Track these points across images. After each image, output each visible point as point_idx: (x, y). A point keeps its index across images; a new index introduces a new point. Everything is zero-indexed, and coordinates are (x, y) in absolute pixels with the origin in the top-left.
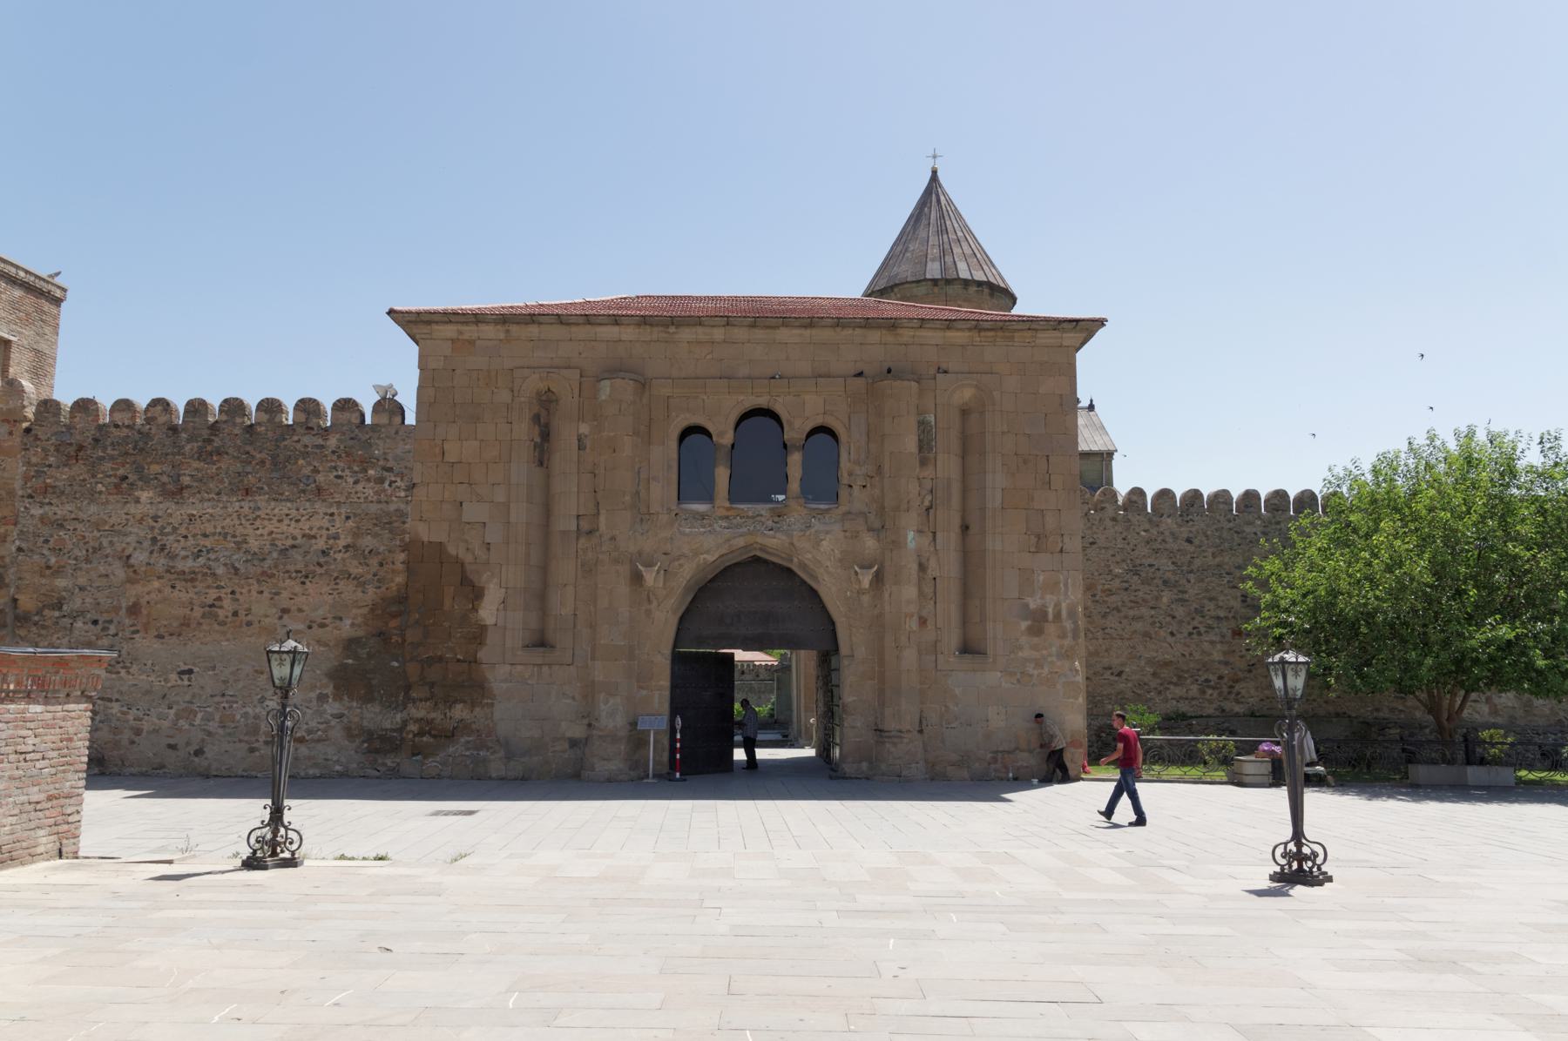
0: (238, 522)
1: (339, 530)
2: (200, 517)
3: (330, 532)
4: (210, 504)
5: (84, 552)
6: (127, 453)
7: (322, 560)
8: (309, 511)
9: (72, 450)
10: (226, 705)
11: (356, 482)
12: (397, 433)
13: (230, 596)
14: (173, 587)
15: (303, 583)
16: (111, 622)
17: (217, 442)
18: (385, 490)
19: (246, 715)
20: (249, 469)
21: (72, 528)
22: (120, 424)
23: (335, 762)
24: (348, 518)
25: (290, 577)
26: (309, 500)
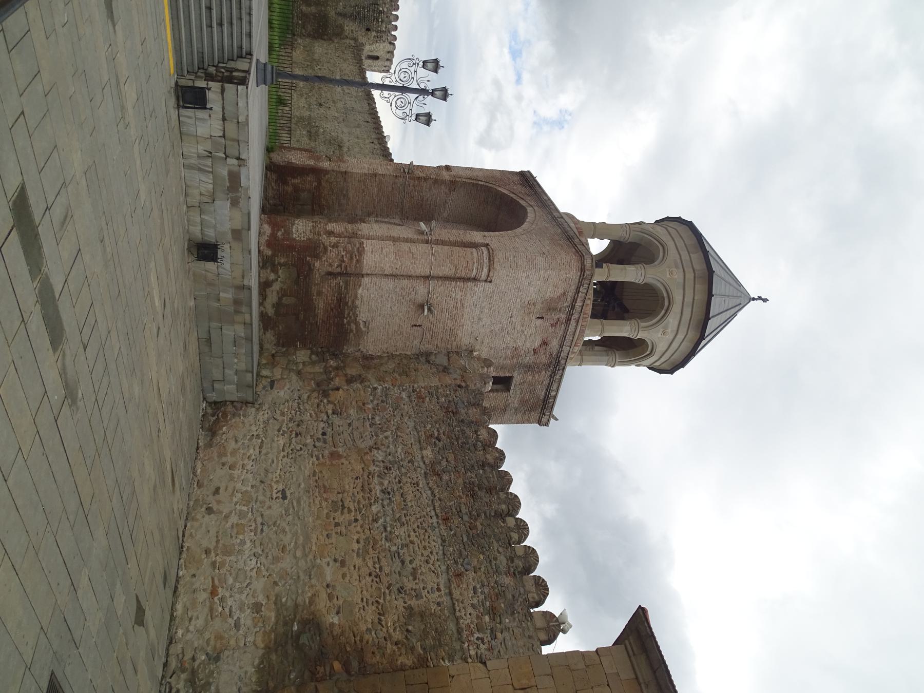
0: (418, 516)
1: (425, 599)
2: (418, 490)
3: (422, 591)
4: (430, 495)
5: (378, 422)
6: (457, 439)
7: (394, 589)
8: (439, 569)
9: (452, 408)
10: (253, 528)
11: (473, 606)
12: (530, 637)
13: (353, 518)
14: (357, 478)
15: (370, 575)
16: (325, 442)
17: (481, 494)
18: (472, 634)
19: (243, 543)
20: (466, 518)
21: (395, 414)
22: (479, 433)
23: (187, 628)
24: (439, 604)
25: (374, 563)
26: (448, 568)
